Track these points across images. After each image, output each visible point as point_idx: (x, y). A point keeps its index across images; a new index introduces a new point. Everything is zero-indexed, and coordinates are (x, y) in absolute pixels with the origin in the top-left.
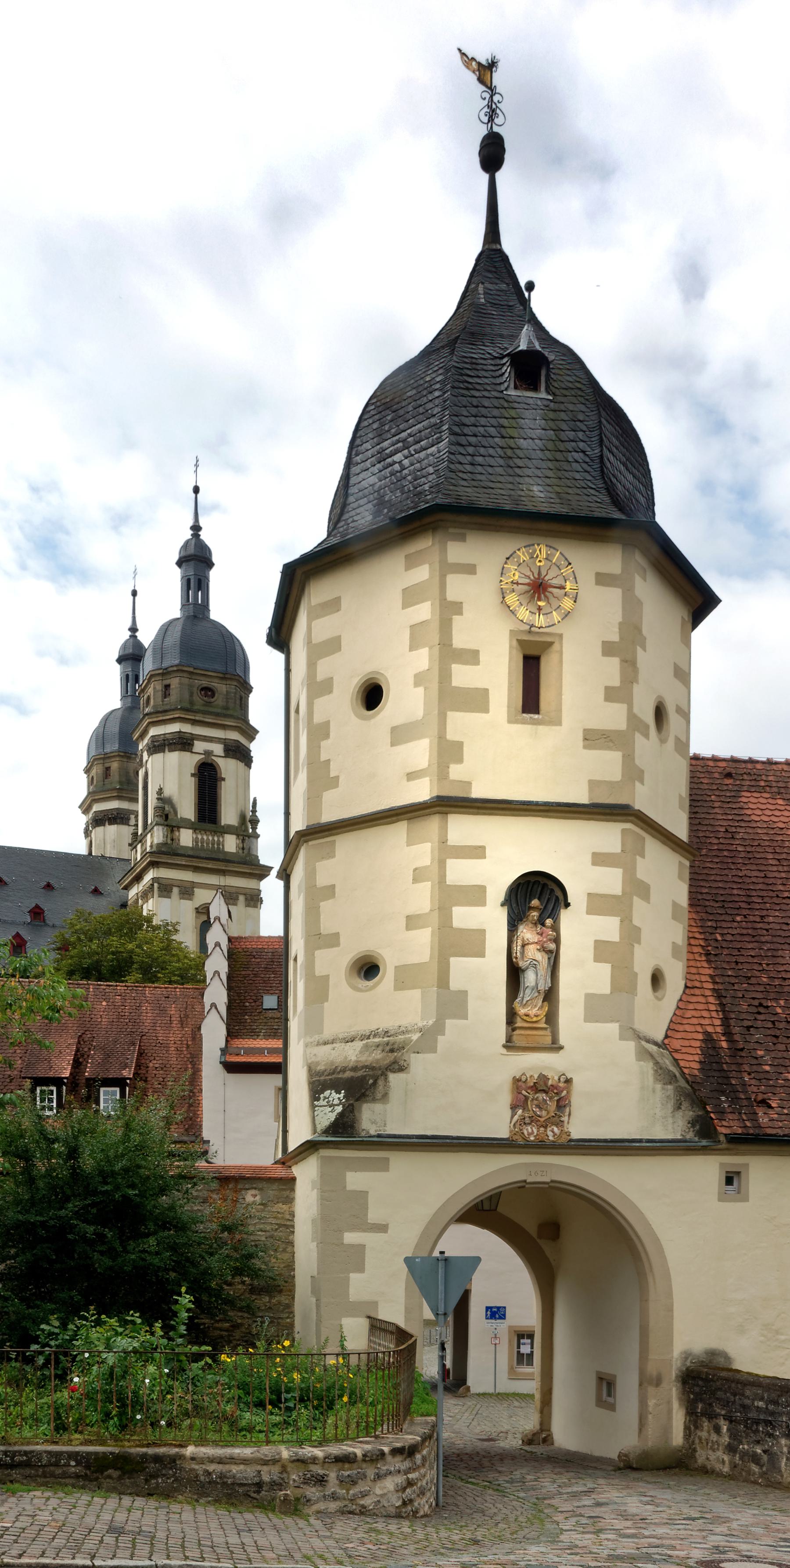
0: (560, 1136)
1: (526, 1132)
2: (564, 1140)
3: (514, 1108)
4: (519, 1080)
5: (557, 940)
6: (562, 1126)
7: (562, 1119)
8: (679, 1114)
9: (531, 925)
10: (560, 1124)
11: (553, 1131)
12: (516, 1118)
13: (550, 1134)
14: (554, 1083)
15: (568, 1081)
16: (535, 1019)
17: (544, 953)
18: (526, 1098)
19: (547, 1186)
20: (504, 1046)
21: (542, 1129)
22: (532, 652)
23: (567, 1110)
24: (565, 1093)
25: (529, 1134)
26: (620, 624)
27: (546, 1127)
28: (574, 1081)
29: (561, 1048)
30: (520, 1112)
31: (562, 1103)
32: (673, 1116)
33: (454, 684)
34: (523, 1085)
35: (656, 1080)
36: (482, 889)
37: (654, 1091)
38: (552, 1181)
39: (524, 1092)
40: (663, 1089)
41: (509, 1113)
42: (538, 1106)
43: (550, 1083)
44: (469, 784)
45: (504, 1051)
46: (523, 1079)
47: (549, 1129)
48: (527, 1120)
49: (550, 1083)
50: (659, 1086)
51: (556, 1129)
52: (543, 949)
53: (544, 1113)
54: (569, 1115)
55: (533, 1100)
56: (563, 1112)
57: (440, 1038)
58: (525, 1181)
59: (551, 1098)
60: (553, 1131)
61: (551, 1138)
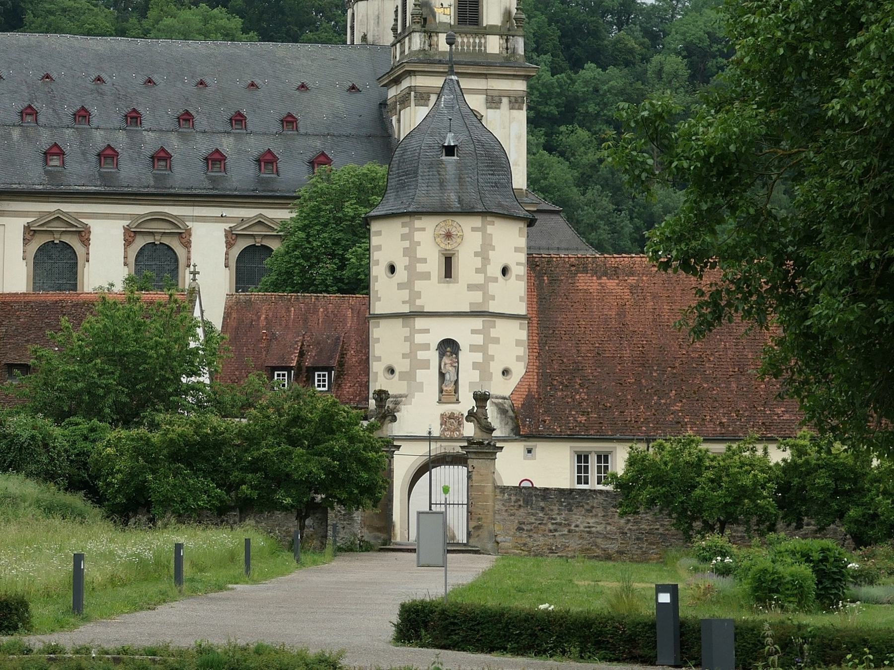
2: (461, 437)
3: (441, 425)
5: (458, 362)
8: (507, 426)
50: (499, 416)
52: (452, 366)
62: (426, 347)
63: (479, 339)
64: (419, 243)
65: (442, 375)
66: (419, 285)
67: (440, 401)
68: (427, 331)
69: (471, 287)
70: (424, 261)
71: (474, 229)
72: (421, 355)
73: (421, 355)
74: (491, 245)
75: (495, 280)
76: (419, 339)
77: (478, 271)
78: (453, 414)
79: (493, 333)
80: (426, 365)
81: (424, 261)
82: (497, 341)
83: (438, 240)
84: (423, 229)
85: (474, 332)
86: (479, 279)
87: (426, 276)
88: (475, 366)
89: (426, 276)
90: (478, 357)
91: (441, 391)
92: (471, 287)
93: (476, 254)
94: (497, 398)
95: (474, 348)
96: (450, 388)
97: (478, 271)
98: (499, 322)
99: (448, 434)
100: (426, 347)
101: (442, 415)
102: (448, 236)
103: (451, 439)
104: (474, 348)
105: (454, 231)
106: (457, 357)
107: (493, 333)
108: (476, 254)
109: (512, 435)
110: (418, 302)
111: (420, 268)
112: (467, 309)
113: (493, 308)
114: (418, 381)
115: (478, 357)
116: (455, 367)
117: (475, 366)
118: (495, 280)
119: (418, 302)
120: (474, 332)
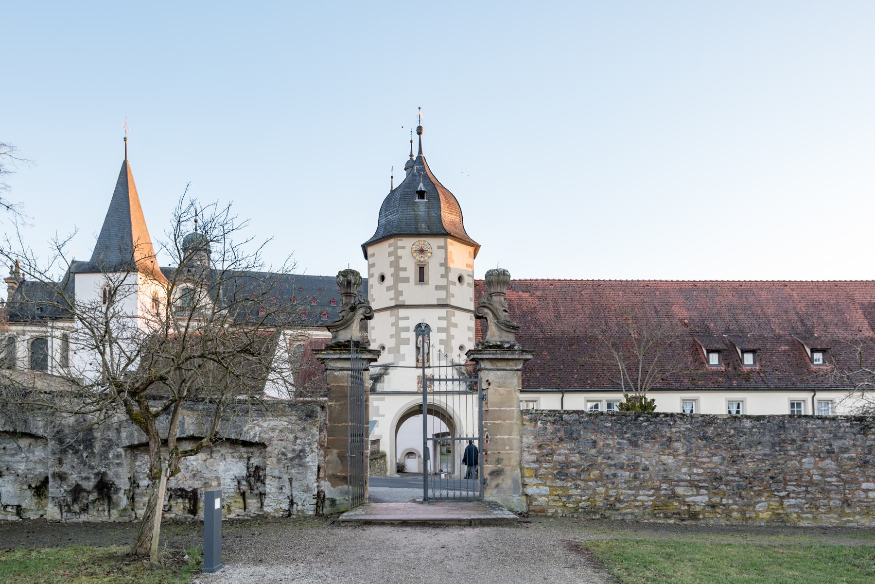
3: (418, 383)
10: (431, 387)
44: (404, 301)
62: (407, 329)
63: (443, 324)
66: (401, 286)
68: (407, 318)
69: (438, 288)
70: (405, 269)
71: (439, 247)
72: (404, 335)
73: (404, 335)
76: (402, 324)
77: (442, 276)
80: (406, 342)
81: (405, 269)
83: (414, 254)
84: (404, 247)
85: (440, 318)
86: (443, 282)
87: (406, 280)
88: (441, 342)
90: (443, 336)
92: (438, 288)
95: (440, 330)
97: (442, 276)
98: (457, 312)
100: (407, 329)
102: (422, 251)
104: (440, 330)
108: (441, 265)
110: (401, 298)
112: (435, 303)
113: (453, 302)
114: (401, 353)
117: (441, 342)
118: (454, 284)
119: (401, 298)
120: (440, 318)
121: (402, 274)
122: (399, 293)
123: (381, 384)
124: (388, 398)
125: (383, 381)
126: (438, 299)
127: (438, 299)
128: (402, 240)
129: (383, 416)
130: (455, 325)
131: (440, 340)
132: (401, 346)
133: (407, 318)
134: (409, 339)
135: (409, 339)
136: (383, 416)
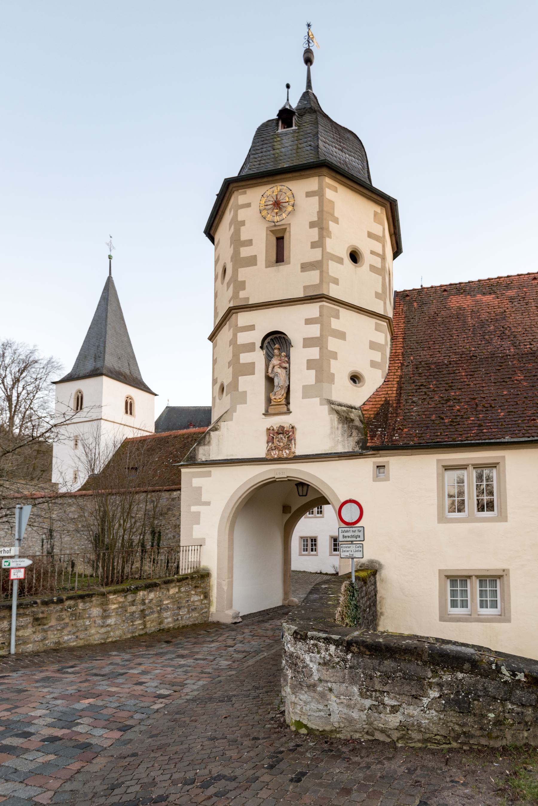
0: (289, 454)
1: (272, 454)
2: (291, 456)
3: (268, 442)
4: (270, 429)
5: (289, 362)
6: (290, 450)
7: (291, 446)
8: (351, 438)
9: (276, 357)
10: (289, 449)
11: (285, 452)
12: (268, 447)
13: (284, 454)
14: (288, 429)
15: (293, 428)
16: (279, 400)
17: (282, 369)
18: (273, 438)
19: (286, 479)
20: (264, 414)
21: (281, 452)
22: (279, 235)
23: (293, 441)
24: (291, 434)
25: (274, 455)
26: (318, 212)
27: (282, 451)
28: (296, 426)
29: (291, 412)
30: (270, 444)
31: (290, 438)
32: (348, 440)
33: (242, 256)
34: (271, 431)
35: (339, 423)
36: (254, 344)
37: (338, 428)
38: (288, 477)
39: (271, 435)
40: (342, 427)
41: (266, 445)
42: (278, 441)
43: (285, 429)
45: (264, 417)
46: (271, 429)
47: (284, 451)
48: (273, 448)
49: (285, 429)
50: (340, 426)
51: (287, 451)
52: (281, 367)
53: (282, 444)
54: (295, 444)
55: (276, 438)
56: (291, 443)
57: (234, 414)
58: (274, 478)
59: (285, 437)
60: (285, 452)
61: (285, 456)
62: (250, 348)
63: (315, 331)
64: (243, 223)
65: (270, 380)
66: (244, 273)
67: (267, 414)
68: (251, 328)
69: (305, 267)
70: (249, 243)
71: (309, 194)
72: (245, 358)
73: (245, 358)
74: (332, 215)
75: (340, 261)
76: (243, 338)
77: (314, 245)
78: (282, 428)
79: (335, 324)
80: (249, 369)
81: (249, 243)
82: (341, 335)
83: (264, 213)
84: (248, 205)
85: (309, 322)
86: (316, 255)
87: (252, 261)
88: (311, 364)
89: (252, 261)
90: (314, 353)
91: (269, 401)
92: (305, 267)
93: (312, 225)
94: (340, 405)
95: (308, 342)
96: (279, 395)
97: (314, 245)
98: (343, 312)
99: (275, 454)
100: (250, 348)
101: (268, 430)
103: (280, 460)
104: (308, 342)
105: (283, 198)
106: (288, 356)
107: (335, 324)
108: (312, 225)
109: (357, 449)
110: (242, 294)
111: (245, 252)
112: (301, 295)
113: (334, 292)
114: (241, 389)
115: (314, 353)
116: (285, 368)
117: (311, 364)
118: (340, 261)
119: (242, 294)
120: (309, 322)
121: (245, 252)
122: (242, 285)
123: (206, 447)
124: (216, 471)
125: (209, 442)
126: (305, 288)
127: (305, 288)
128: (245, 193)
129: (208, 504)
130: (341, 335)
131: (308, 361)
132: (240, 378)
133: (251, 328)
134: (252, 365)
135: (252, 365)
136: (208, 504)
